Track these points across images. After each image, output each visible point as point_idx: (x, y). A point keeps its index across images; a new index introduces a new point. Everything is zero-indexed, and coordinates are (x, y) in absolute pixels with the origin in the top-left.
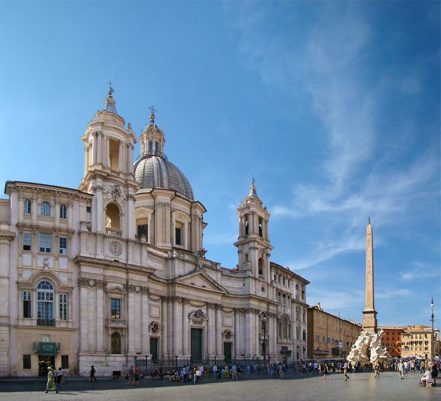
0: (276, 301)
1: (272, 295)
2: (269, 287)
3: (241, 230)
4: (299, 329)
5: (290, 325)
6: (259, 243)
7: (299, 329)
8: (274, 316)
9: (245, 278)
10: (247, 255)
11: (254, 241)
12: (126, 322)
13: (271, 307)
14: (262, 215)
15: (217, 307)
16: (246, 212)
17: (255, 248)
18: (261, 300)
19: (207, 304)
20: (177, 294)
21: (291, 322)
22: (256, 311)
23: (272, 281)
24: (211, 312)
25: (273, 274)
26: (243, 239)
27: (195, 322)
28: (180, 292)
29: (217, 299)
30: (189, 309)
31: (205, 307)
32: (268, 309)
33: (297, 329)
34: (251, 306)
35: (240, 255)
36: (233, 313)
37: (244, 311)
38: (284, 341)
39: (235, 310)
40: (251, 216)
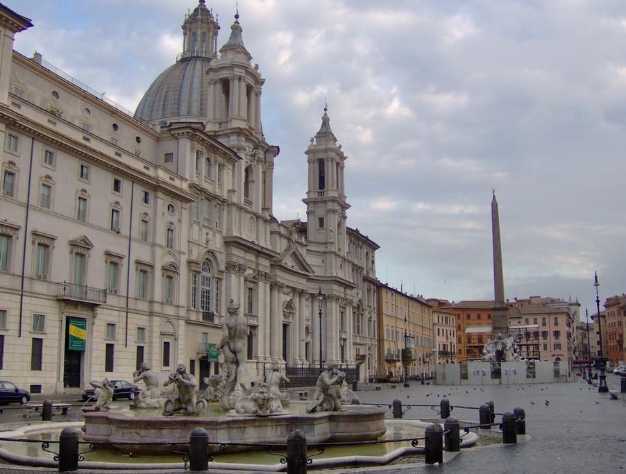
0: (352, 281)
1: (346, 275)
2: (347, 263)
4: (370, 320)
5: (362, 314)
6: (339, 204)
7: (370, 320)
8: (351, 302)
9: (325, 253)
10: (321, 221)
12: (256, 316)
13: (348, 291)
14: (338, 159)
15: (302, 293)
16: (321, 156)
17: (334, 212)
18: (342, 283)
19: (294, 289)
20: (278, 279)
21: (363, 310)
22: (337, 298)
23: (347, 253)
24: (297, 300)
25: (347, 242)
27: (285, 315)
28: (282, 277)
29: (301, 283)
31: (291, 294)
33: (368, 320)
34: (334, 293)
35: (312, 217)
36: (310, 300)
37: (326, 298)
38: (358, 341)
39: (312, 296)
40: (330, 163)
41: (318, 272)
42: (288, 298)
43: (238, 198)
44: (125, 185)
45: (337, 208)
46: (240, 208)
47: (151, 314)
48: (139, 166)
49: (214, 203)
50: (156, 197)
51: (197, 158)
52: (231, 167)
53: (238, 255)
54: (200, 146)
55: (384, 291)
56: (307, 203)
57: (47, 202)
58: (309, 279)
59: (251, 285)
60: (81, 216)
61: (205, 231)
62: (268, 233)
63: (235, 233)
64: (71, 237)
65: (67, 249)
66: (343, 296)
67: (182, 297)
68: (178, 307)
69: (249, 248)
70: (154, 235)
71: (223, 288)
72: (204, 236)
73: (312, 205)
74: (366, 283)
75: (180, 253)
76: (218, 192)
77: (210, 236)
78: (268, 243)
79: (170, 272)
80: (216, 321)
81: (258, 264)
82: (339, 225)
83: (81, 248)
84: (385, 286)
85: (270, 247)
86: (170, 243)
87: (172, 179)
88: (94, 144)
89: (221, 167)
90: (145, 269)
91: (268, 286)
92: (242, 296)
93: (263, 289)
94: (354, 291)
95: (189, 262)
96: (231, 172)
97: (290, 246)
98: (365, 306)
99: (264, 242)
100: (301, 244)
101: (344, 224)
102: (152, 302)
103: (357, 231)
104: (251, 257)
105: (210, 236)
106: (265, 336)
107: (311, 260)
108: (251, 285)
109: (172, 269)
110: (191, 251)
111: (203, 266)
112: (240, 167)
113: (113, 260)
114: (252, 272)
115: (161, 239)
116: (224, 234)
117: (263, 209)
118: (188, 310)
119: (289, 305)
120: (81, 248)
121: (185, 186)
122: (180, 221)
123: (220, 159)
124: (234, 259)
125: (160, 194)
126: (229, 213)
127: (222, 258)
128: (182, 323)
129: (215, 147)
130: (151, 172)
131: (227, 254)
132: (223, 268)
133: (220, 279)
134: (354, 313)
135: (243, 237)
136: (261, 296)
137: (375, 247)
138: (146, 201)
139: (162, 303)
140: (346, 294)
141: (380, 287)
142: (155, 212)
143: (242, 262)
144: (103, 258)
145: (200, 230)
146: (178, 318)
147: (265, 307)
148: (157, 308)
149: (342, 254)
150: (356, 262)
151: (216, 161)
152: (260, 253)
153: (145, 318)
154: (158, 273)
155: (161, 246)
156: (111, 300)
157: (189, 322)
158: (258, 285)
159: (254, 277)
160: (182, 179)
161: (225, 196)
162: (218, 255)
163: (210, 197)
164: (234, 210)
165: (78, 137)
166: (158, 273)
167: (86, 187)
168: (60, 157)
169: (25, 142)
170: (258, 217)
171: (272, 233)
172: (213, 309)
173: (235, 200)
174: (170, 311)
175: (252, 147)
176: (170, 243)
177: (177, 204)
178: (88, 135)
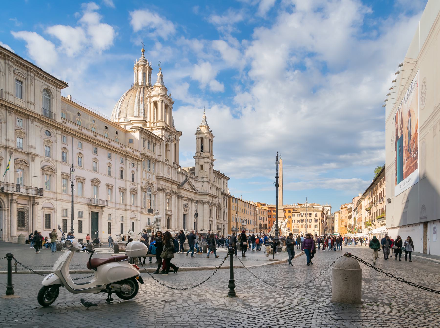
1: (213, 192)
3: (197, 147)
8: (215, 204)
10: (202, 166)
11: (208, 158)
13: (214, 199)
15: (192, 200)
19: (189, 198)
20: (181, 194)
22: (208, 203)
24: (190, 203)
25: (214, 176)
26: (199, 154)
27: (184, 210)
28: (183, 193)
29: (192, 196)
30: (184, 202)
32: (213, 201)
35: (197, 165)
37: (203, 203)
39: (197, 202)
41: (200, 190)
42: (186, 202)
43: (163, 158)
44: (113, 155)
45: (209, 160)
46: (164, 163)
47: (126, 210)
48: (118, 146)
49: (151, 161)
50: (126, 160)
51: (144, 141)
52: (159, 144)
53: (163, 184)
54: (145, 136)
55: (231, 199)
56: (195, 158)
57: (80, 164)
58: (196, 194)
59: (169, 197)
60: (95, 170)
61: (148, 174)
62: (176, 173)
63: (161, 175)
64: (92, 178)
65: (90, 183)
66: (211, 201)
67: (139, 202)
68: (137, 207)
69: (168, 181)
70: (126, 177)
71: (156, 199)
72: (148, 176)
73: (197, 159)
74: (223, 196)
75: (137, 184)
76: (153, 156)
77: (151, 175)
78: (176, 178)
79: (133, 192)
80: (154, 212)
81: (172, 188)
82: (210, 169)
83: (96, 182)
84: (233, 197)
85: (177, 181)
86: (133, 179)
87: (133, 152)
88: (99, 138)
89: (155, 145)
90: (123, 191)
91: (176, 197)
92: (165, 202)
93: (174, 199)
94: (217, 199)
95: (142, 188)
96: (159, 147)
97: (186, 179)
98: (222, 206)
99: (174, 177)
100: (192, 178)
101: (212, 168)
102: (126, 205)
103: (219, 172)
104: (169, 185)
105: (150, 177)
106: (175, 219)
107: (197, 185)
108: (169, 197)
109: (134, 191)
110: (142, 183)
111: (147, 189)
112: (163, 144)
113: (109, 187)
114: (169, 191)
115: (129, 178)
116: (156, 175)
117: (174, 163)
118: (141, 208)
119: (186, 206)
120: (96, 182)
121: (138, 154)
122: (137, 170)
123: (154, 141)
124: (161, 186)
125: (128, 159)
126: (158, 165)
127: (155, 185)
128: (139, 214)
129: (151, 136)
130: (124, 149)
131: (158, 184)
132: (156, 190)
133: (155, 195)
134: (217, 209)
135: (165, 176)
136: (173, 201)
137: (227, 179)
138: (122, 162)
139: (131, 206)
140: (213, 201)
141: (229, 197)
142: (126, 166)
143: (165, 187)
144: (105, 186)
145: (146, 173)
146: (137, 211)
147: (175, 207)
148: (128, 207)
149: (211, 183)
150: (219, 186)
151: (152, 142)
152: (173, 183)
153: (124, 212)
154: (128, 192)
155: (129, 181)
156: (109, 204)
157: (141, 212)
158: (172, 197)
159: (170, 194)
160: (137, 151)
161: (157, 157)
162: (154, 184)
163: (150, 159)
164: (160, 164)
165: (92, 135)
166: (128, 192)
167: (96, 157)
168: (85, 144)
169: (70, 138)
170: (172, 167)
171: (178, 173)
172: (152, 208)
173: (161, 160)
174: (134, 208)
175: (168, 134)
176: (133, 179)
177: (135, 162)
178: (96, 134)
